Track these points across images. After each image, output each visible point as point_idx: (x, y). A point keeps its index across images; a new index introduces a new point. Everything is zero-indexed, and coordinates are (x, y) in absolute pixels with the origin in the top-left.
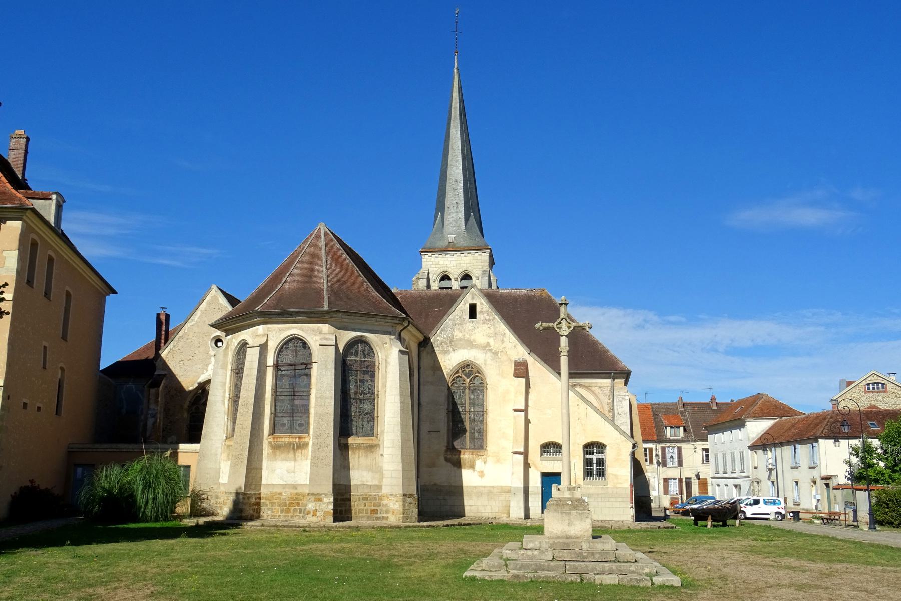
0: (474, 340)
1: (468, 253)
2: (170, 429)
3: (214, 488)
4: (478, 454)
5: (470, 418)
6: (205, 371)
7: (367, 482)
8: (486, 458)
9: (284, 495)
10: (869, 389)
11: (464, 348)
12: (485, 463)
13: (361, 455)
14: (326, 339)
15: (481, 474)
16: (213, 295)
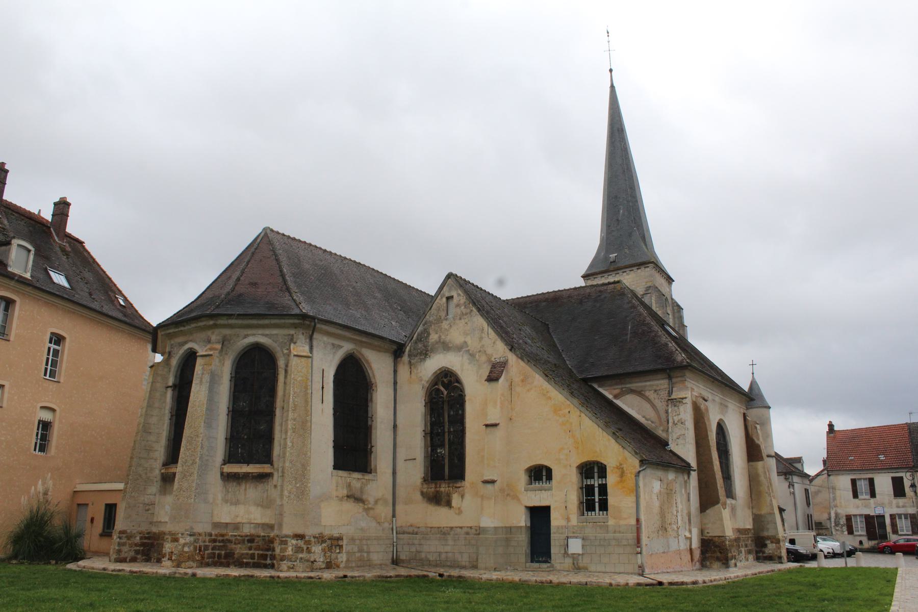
1: (630, 271)
7: (254, 519)
8: (464, 490)
11: (439, 353)
12: (462, 496)
13: (248, 487)
15: (460, 511)
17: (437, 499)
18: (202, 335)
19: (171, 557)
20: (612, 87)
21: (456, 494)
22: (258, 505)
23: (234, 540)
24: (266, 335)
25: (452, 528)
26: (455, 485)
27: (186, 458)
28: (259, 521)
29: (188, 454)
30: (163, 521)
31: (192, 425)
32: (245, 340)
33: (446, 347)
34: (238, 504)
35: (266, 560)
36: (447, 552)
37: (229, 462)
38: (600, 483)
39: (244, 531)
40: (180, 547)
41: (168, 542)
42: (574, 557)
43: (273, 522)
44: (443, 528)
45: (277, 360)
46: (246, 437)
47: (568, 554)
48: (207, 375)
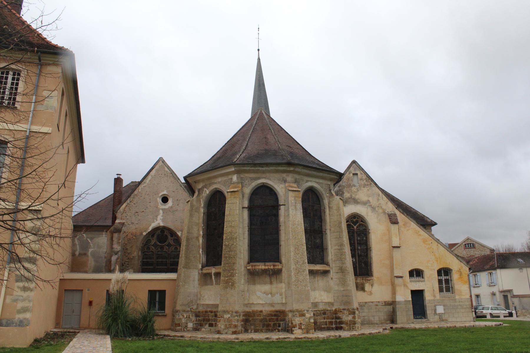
0: (358, 199)
2: (128, 264)
3: (194, 309)
4: (367, 279)
6: (155, 221)
8: (373, 282)
9: (264, 313)
10: (466, 247)
11: (352, 204)
12: (372, 285)
13: (319, 279)
15: (371, 293)
16: (160, 165)
17: (360, 288)
18: (277, 175)
19: (301, 327)
20: (259, 59)
21: (368, 284)
22: (325, 291)
24: (317, 183)
25: (366, 303)
26: (367, 279)
27: (297, 259)
28: (327, 301)
29: (298, 257)
30: (255, 303)
31: (296, 237)
32: (307, 183)
33: (356, 202)
36: (364, 316)
37: (250, 262)
38: (445, 278)
39: (320, 308)
40: (307, 320)
41: (297, 317)
42: (440, 315)
44: (360, 303)
45: (323, 200)
46: (310, 247)
47: (436, 314)
48: (299, 204)
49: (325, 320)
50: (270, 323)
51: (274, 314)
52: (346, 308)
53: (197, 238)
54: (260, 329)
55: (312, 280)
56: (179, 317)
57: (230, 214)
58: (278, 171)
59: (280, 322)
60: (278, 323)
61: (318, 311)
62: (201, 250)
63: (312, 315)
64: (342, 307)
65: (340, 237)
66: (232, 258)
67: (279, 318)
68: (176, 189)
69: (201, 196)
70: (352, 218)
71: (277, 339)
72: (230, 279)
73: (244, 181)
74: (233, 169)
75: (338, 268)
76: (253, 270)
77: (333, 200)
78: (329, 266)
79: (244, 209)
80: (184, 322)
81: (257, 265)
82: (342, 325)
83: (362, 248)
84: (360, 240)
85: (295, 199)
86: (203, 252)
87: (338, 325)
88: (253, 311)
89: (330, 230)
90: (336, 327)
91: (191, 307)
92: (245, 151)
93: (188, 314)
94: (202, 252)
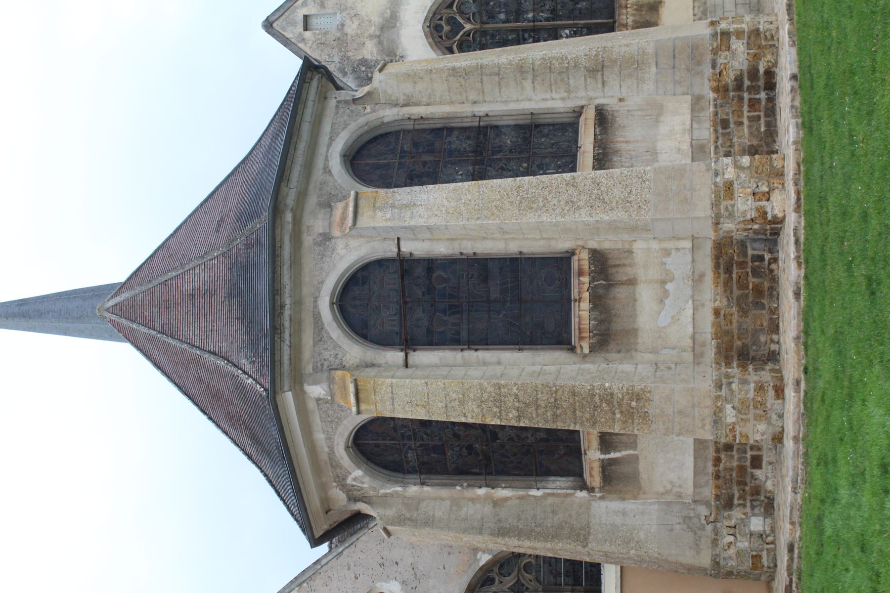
5: (547, 20)
13: (622, 139)
14: (344, 218)
18: (309, 261)
22: (657, 121)
23: (725, 149)
24: (332, 140)
28: (687, 118)
29: (555, 202)
31: (496, 207)
32: (333, 172)
34: (655, 150)
35: (760, 99)
36: (736, 5)
37: (570, 343)
39: (707, 137)
40: (743, 176)
41: (733, 206)
43: (688, 98)
44: (694, 15)
45: (383, 123)
46: (525, 165)
48: (397, 196)
49: (746, 121)
50: (751, 286)
51: (725, 273)
52: (709, 57)
53: (497, 503)
54: (767, 317)
55: (624, 160)
56: (735, 558)
57: (426, 406)
58: (296, 262)
59: (749, 258)
60: (753, 262)
61: (716, 142)
62: (534, 492)
63: (728, 160)
64: (708, 71)
65: (498, 74)
66: (556, 400)
67: (735, 258)
68: (349, 569)
69: (372, 493)
70: (441, 37)
71: (799, 264)
72: (620, 405)
73: (326, 363)
74: (289, 396)
75: (589, 80)
76: (595, 335)
77: (385, 92)
78: (582, 107)
79: (411, 361)
80: (746, 544)
81: (580, 324)
82: (762, 70)
83: (531, 7)
84: (507, 13)
85: (381, 209)
86: (539, 485)
87: (761, 83)
88: (716, 336)
89: (475, 102)
90: (765, 89)
91: (704, 522)
92: (234, 359)
93: (725, 531)
94: (538, 489)
